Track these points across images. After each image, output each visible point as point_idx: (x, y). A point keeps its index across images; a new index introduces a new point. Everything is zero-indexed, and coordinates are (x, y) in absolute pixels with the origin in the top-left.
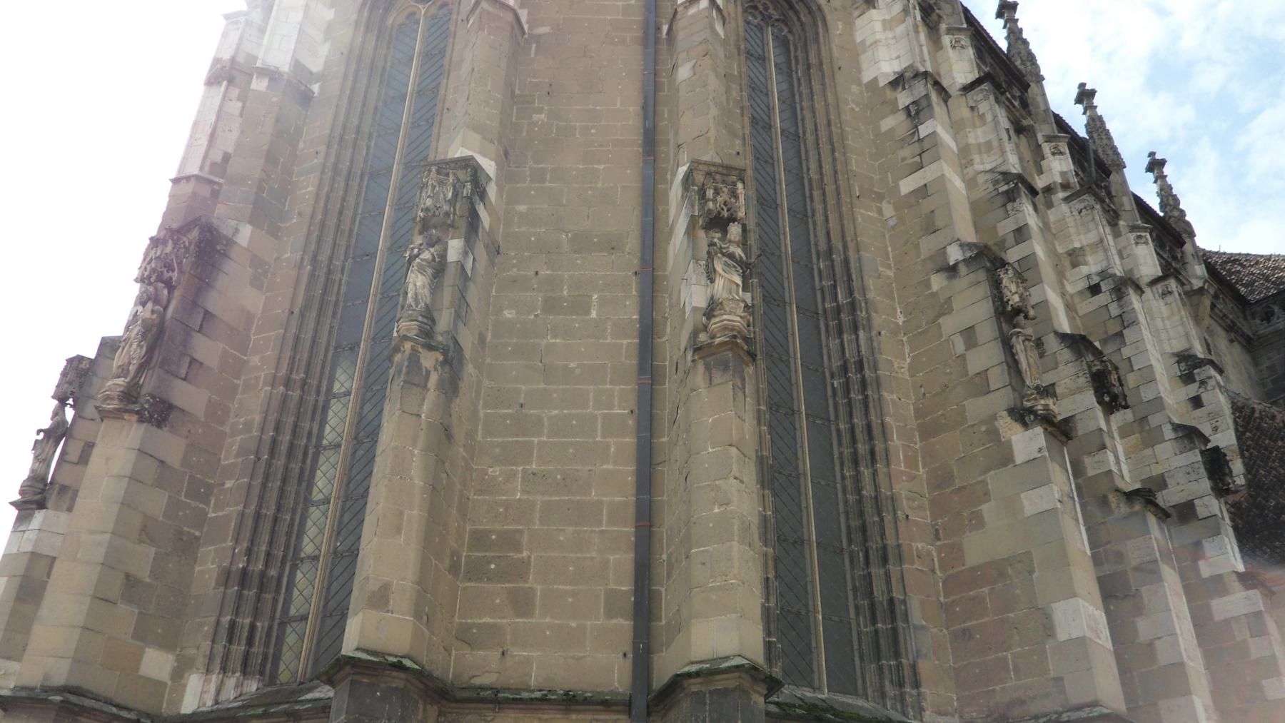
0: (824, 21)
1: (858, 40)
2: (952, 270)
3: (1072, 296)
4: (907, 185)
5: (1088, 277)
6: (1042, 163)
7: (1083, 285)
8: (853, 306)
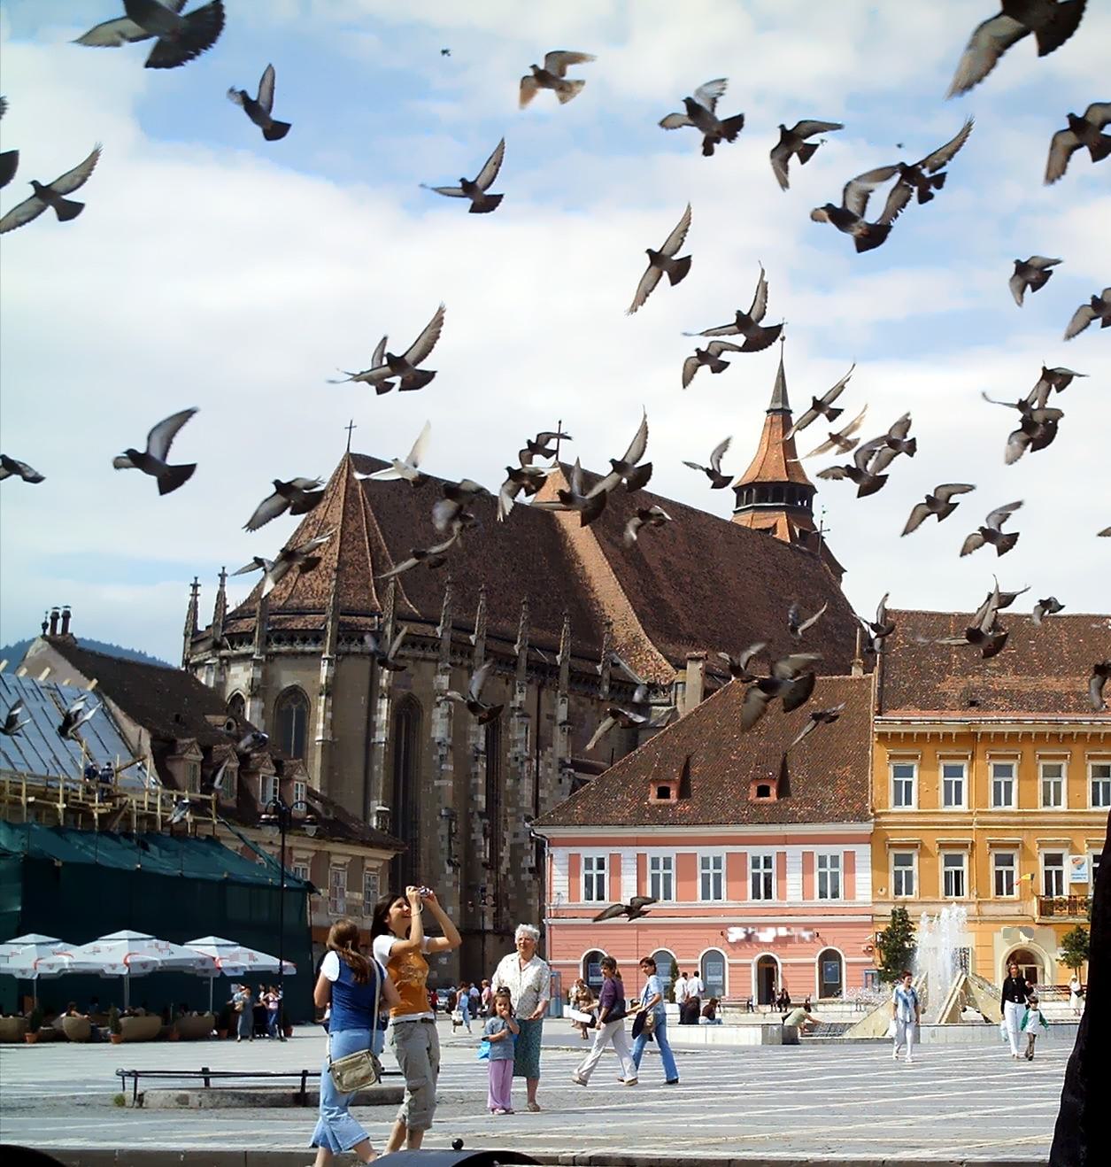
0: (422, 711)
1: (433, 717)
2: (442, 816)
3: (510, 759)
4: (436, 783)
5: (516, 754)
6: (515, 696)
7: (514, 755)
8: (416, 822)
